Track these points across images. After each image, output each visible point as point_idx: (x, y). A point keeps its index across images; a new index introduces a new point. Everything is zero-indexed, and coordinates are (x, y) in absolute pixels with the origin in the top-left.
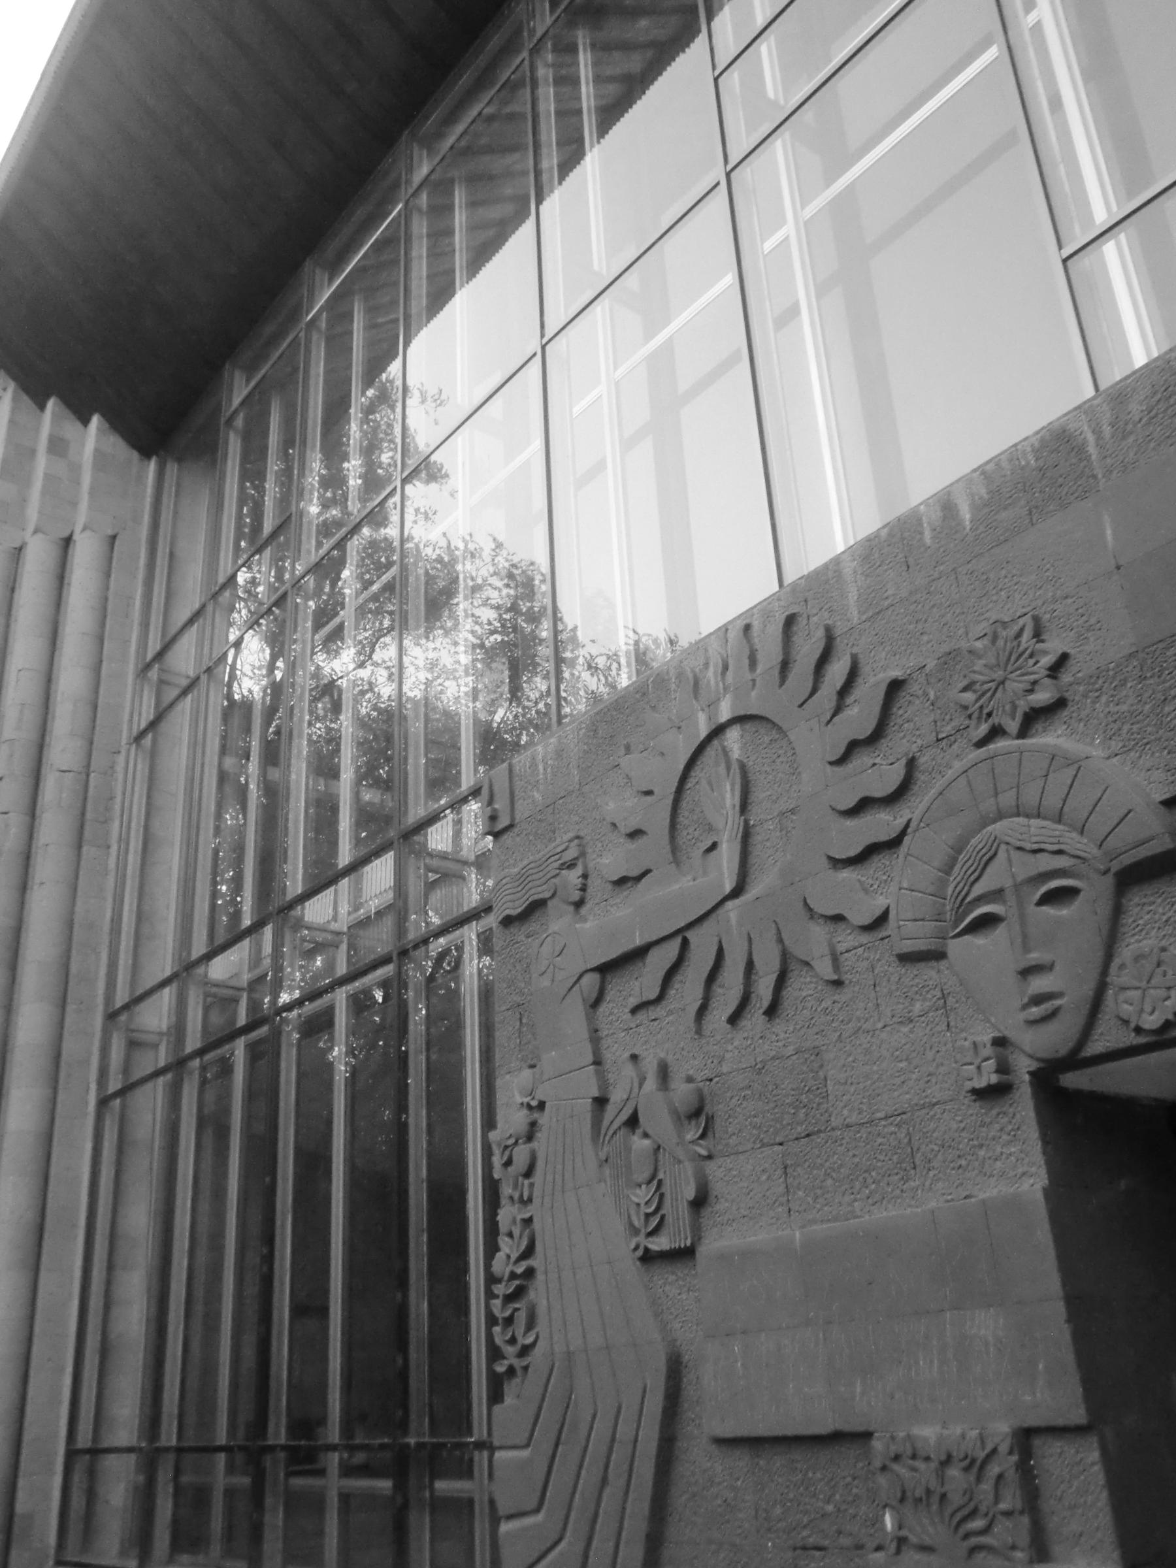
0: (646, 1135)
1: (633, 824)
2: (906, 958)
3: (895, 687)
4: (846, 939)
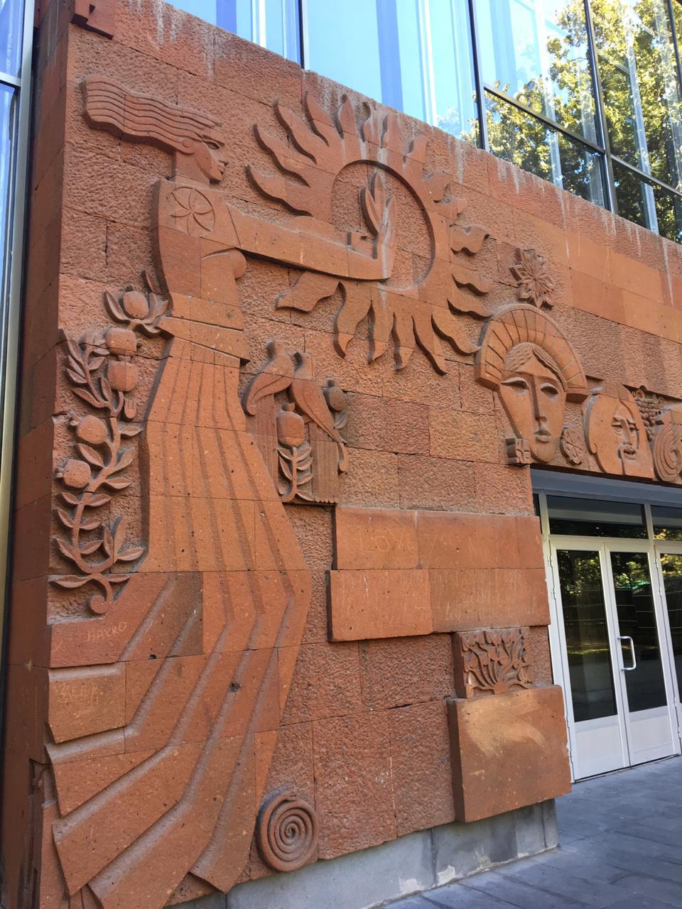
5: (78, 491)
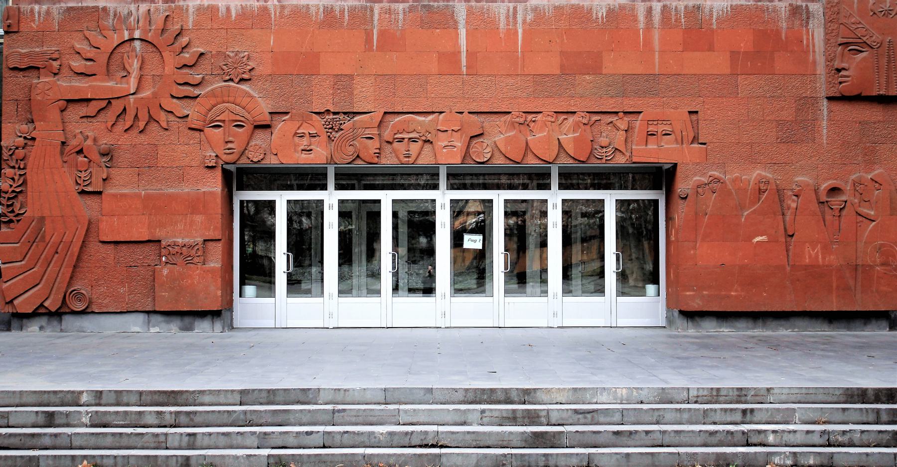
0: (85, 157)
1: (89, 56)
2: (190, 129)
3: (202, 54)
5: (6, 193)
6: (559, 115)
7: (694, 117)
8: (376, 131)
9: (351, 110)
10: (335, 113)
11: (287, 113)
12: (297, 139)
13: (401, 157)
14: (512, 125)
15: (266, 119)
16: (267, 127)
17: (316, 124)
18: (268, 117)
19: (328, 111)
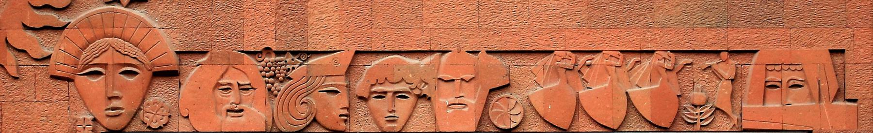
2: (53, 77)
4: (24, 60)
6: (629, 56)
7: (838, 59)
8: (342, 81)
9: (304, 49)
10: (278, 53)
11: (203, 53)
12: (219, 94)
13: (382, 121)
14: (555, 71)
15: (171, 61)
16: (172, 74)
17: (249, 69)
18: (175, 59)
19: (268, 50)
